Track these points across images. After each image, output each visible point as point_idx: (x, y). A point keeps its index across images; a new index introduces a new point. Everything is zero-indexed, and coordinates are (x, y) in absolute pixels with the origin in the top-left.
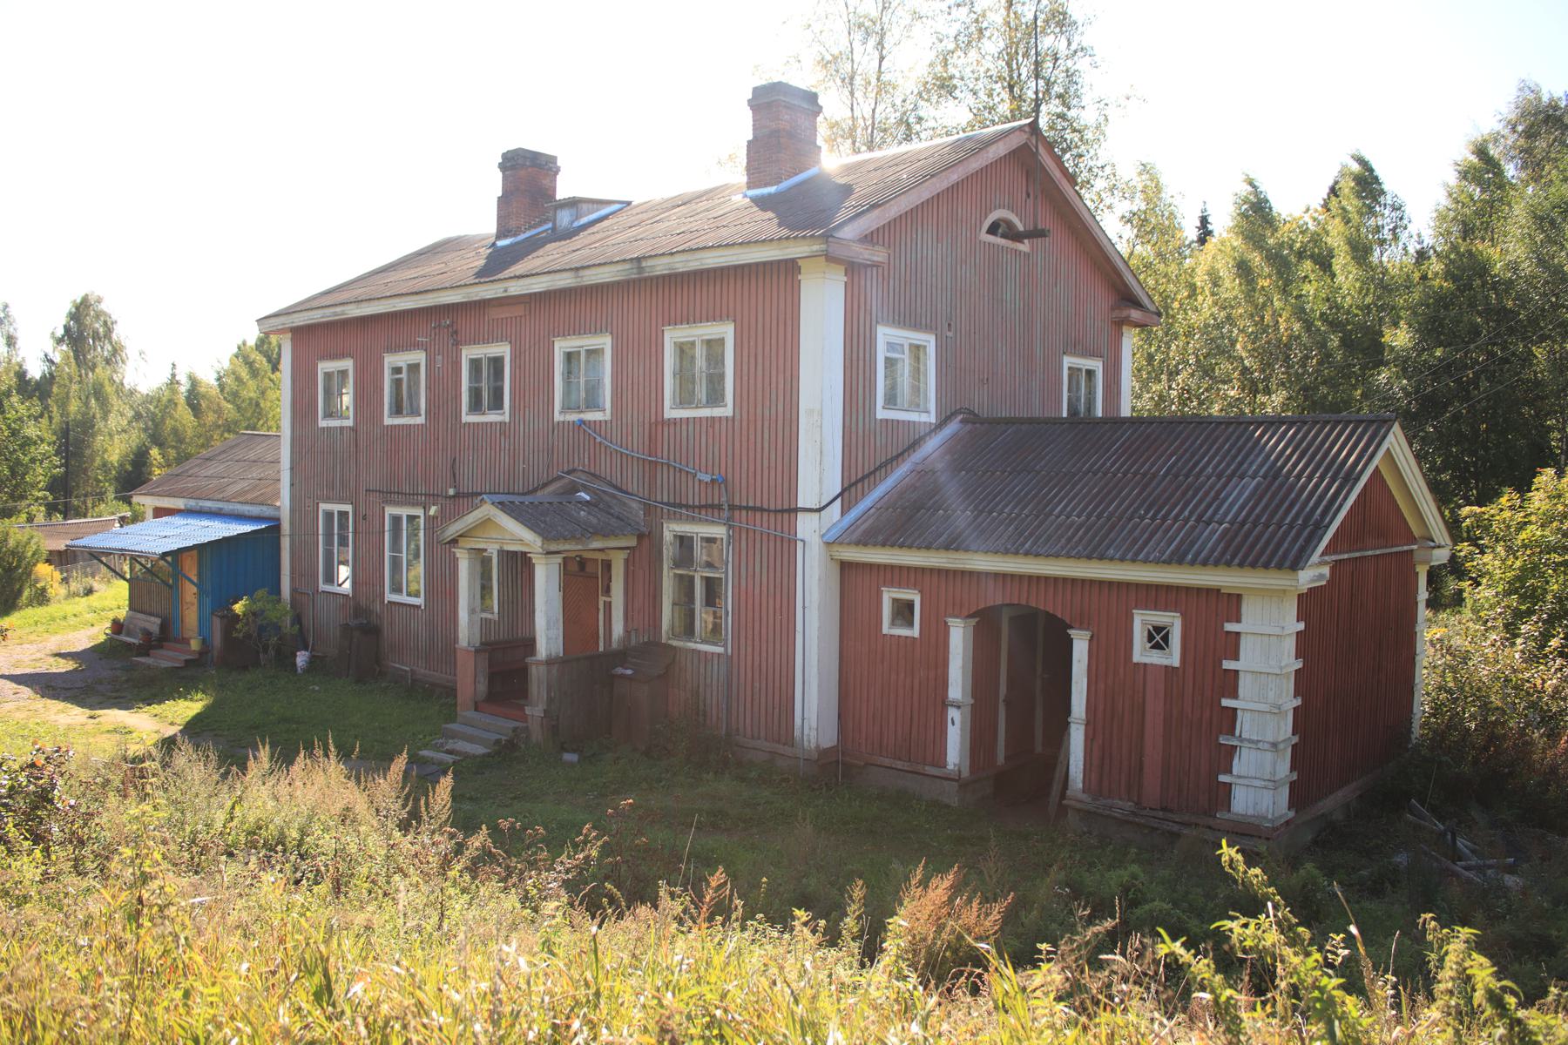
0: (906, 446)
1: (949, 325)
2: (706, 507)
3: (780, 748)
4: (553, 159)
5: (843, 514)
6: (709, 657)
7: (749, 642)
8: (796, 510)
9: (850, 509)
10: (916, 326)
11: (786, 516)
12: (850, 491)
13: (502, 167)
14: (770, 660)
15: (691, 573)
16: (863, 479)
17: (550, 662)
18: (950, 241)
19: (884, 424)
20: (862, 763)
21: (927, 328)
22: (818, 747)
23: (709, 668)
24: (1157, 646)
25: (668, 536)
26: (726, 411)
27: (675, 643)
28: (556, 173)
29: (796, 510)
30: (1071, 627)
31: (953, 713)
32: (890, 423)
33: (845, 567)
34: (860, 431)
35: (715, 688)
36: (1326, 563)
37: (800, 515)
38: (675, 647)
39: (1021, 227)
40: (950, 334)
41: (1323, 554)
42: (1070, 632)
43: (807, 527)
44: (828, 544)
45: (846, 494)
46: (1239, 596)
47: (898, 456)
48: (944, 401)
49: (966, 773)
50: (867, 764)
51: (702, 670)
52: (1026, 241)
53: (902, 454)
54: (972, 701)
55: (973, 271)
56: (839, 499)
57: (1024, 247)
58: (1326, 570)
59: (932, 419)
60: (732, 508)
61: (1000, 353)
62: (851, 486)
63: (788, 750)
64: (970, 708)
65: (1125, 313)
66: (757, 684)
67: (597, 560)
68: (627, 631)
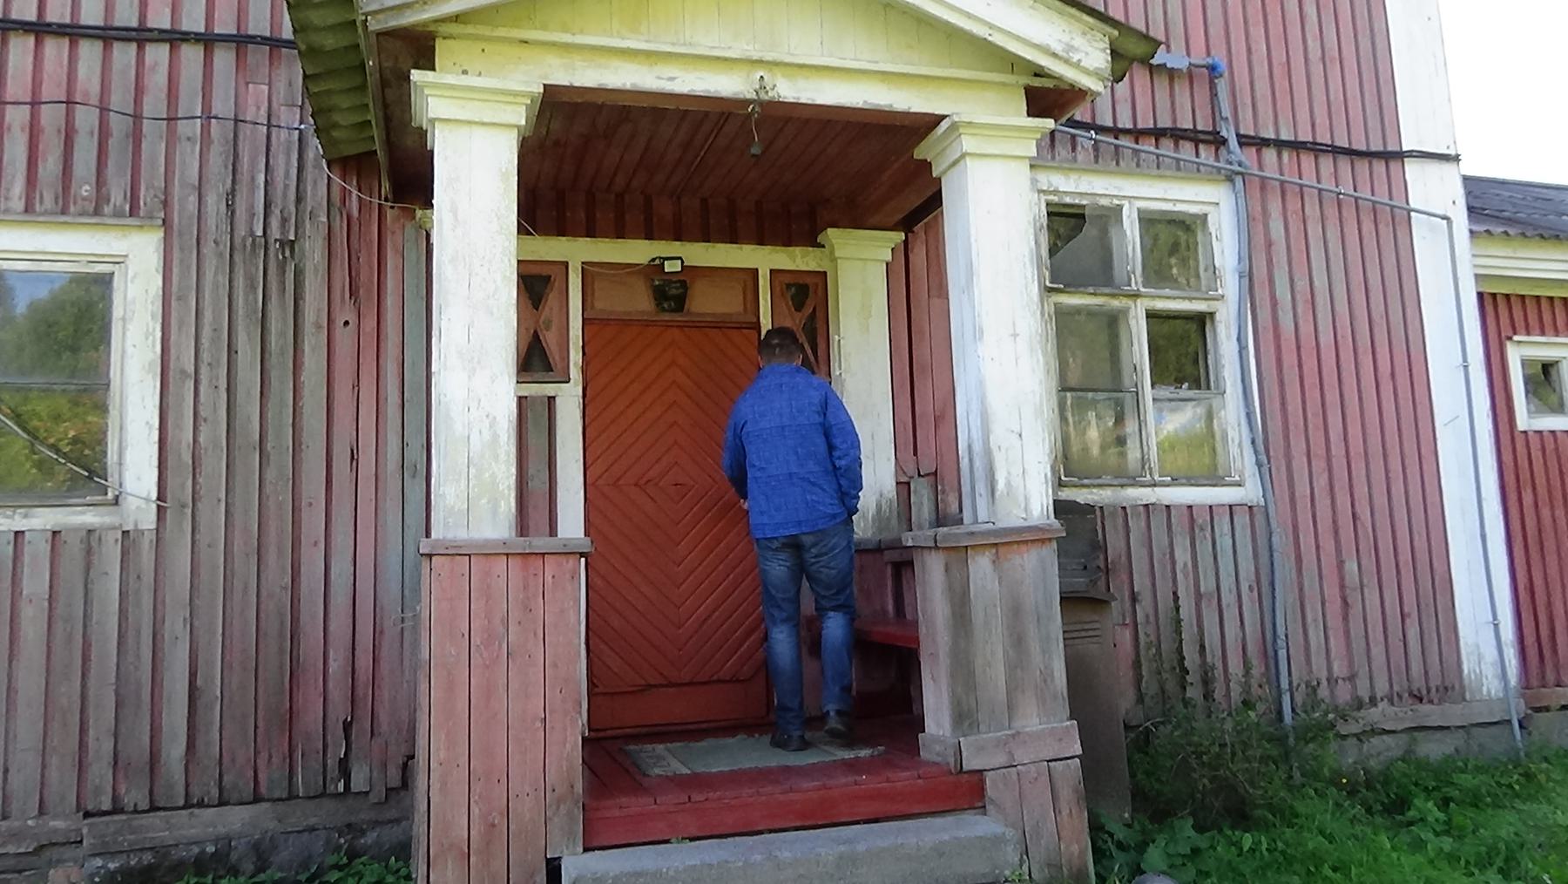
2: (1158, 134)
3: (1432, 714)
6: (1202, 518)
7: (1319, 465)
8: (1401, 156)
11: (1379, 166)
14: (1381, 500)
15: (1116, 303)
23: (1204, 549)
35: (1228, 598)
37: (1412, 169)
38: (1089, 508)
51: (1182, 556)
63: (1451, 714)
66: (1351, 566)
67: (754, 273)
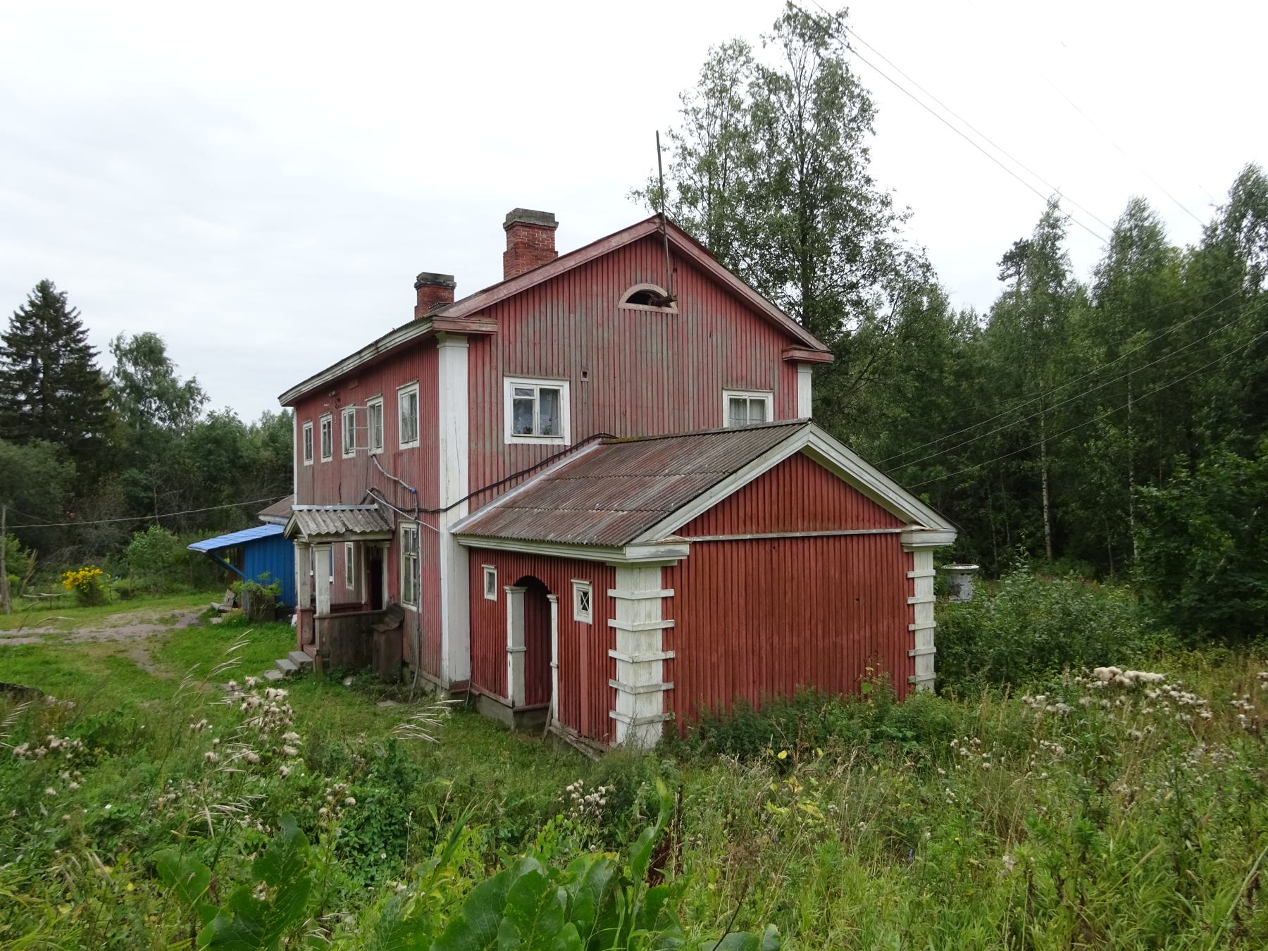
0: (538, 461)
1: (585, 374)
4: (452, 277)
5: (470, 512)
9: (477, 509)
10: (546, 375)
12: (476, 496)
13: (418, 286)
16: (491, 487)
17: (322, 619)
18: (584, 311)
19: (512, 448)
20: (477, 693)
21: (560, 376)
22: (450, 679)
24: (585, 608)
25: (402, 532)
26: (416, 444)
27: (405, 606)
28: (453, 288)
29: (437, 512)
30: (550, 593)
31: (510, 657)
32: (519, 448)
33: (471, 550)
34: (488, 454)
36: (685, 542)
39: (664, 294)
40: (583, 379)
41: (683, 531)
42: (549, 596)
43: (447, 524)
44: (454, 535)
45: (473, 499)
46: (615, 568)
47: (528, 471)
48: (579, 429)
49: (521, 703)
50: (480, 695)
52: (672, 304)
53: (535, 468)
54: (523, 648)
55: (611, 332)
56: (466, 502)
57: (673, 309)
58: (685, 549)
59: (567, 442)
60: (420, 511)
61: (644, 392)
62: (477, 493)
64: (523, 654)
65: (791, 354)
68: (390, 597)
